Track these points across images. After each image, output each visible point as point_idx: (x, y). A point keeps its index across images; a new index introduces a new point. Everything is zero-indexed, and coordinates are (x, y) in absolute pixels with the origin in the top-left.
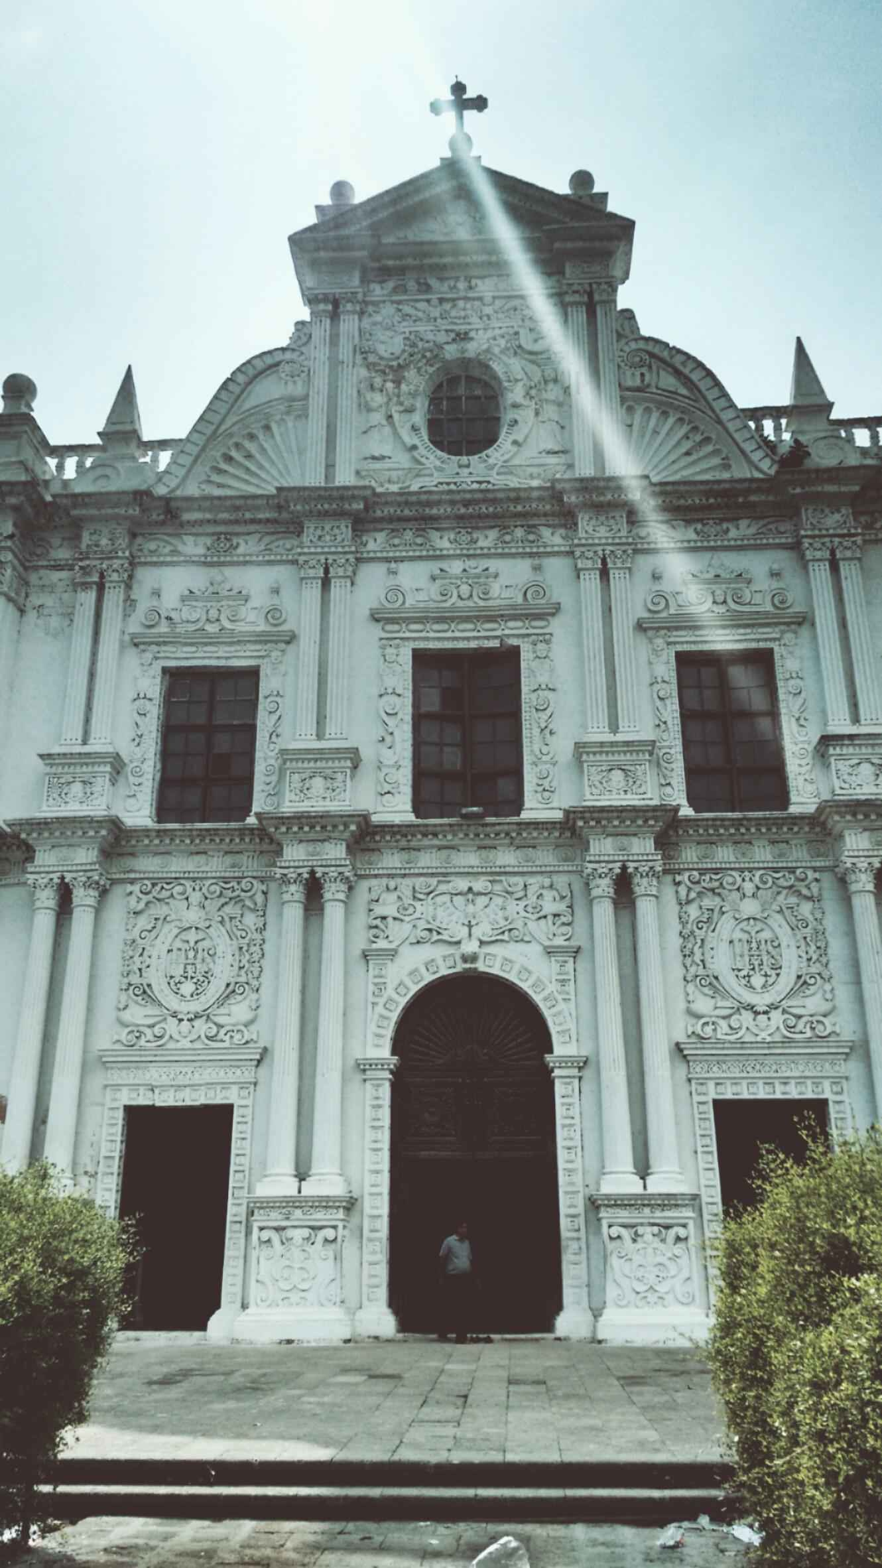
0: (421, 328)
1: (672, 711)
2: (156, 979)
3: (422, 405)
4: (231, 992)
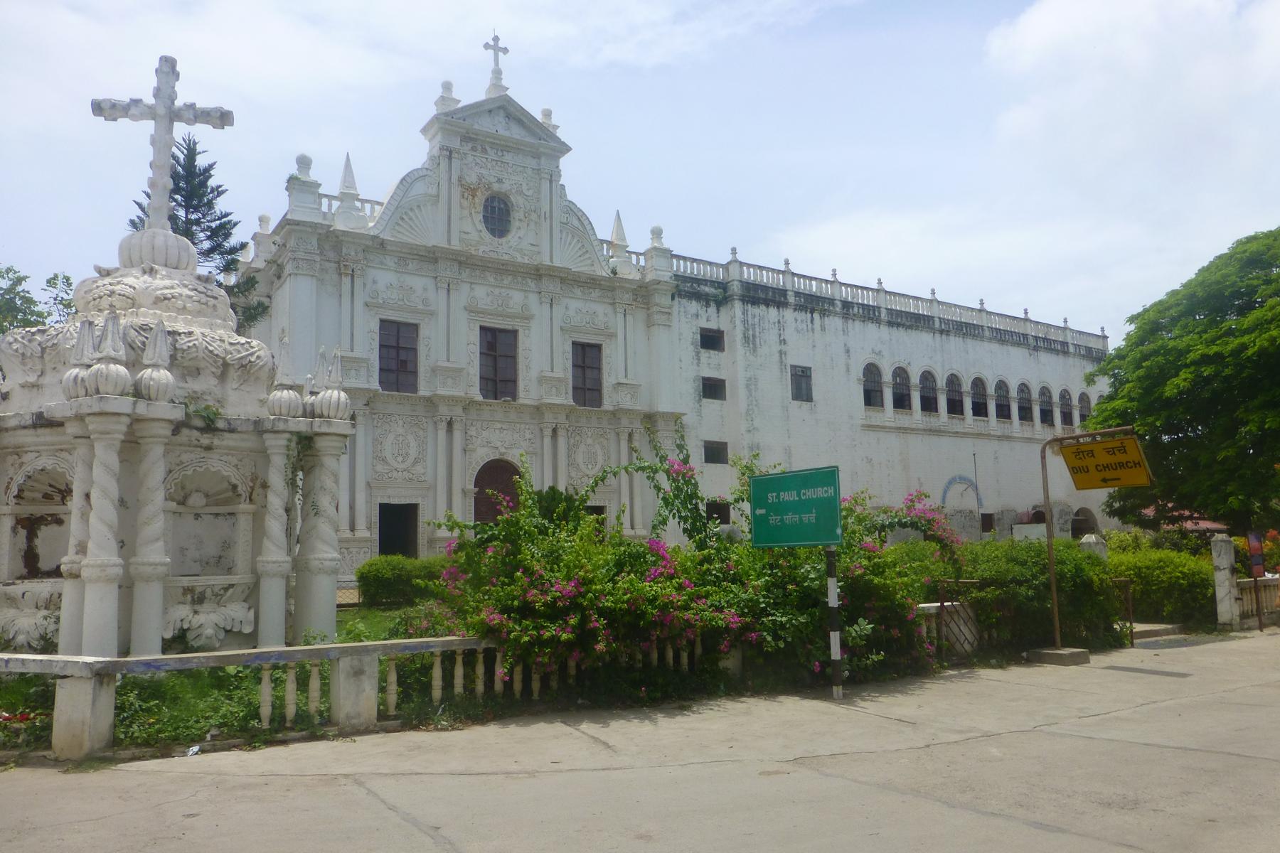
0: (484, 171)
1: (569, 364)
2: (388, 454)
3: (481, 209)
4: (416, 461)
